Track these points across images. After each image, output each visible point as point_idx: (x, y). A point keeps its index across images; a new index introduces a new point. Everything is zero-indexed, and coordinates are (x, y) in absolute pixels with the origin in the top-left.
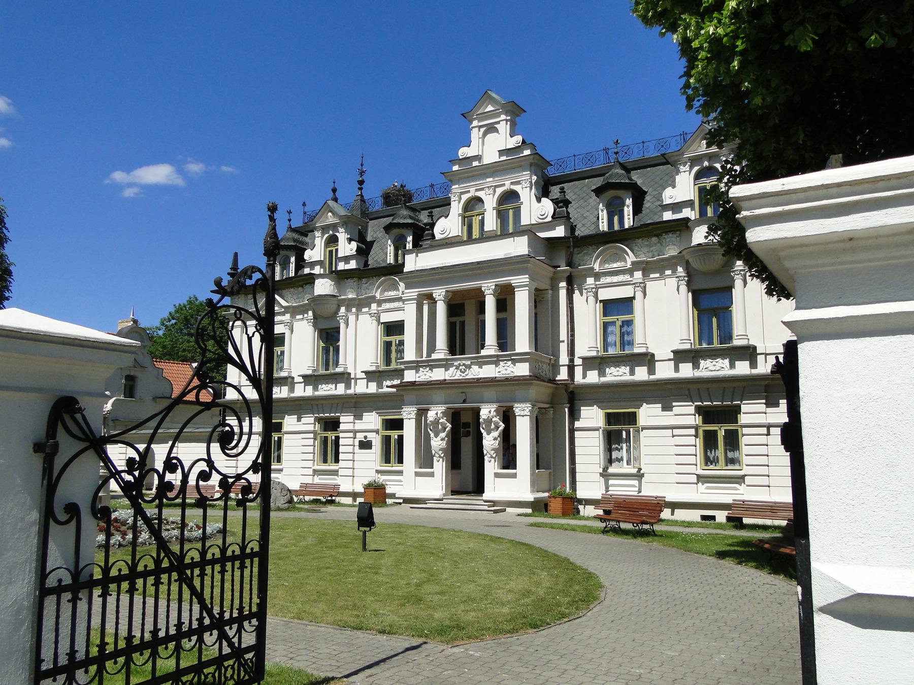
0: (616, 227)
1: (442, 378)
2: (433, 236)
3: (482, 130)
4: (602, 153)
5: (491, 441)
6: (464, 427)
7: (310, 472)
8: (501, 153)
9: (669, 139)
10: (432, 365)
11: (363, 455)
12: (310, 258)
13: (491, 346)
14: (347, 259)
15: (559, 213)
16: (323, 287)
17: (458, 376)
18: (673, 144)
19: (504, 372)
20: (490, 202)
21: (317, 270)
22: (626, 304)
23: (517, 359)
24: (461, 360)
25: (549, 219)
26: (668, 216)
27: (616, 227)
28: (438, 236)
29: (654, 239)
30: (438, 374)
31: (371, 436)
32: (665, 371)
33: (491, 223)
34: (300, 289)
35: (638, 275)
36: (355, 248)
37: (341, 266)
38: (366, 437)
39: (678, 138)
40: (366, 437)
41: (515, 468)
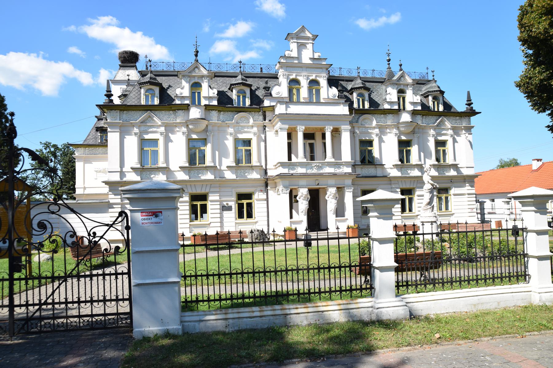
0: (361, 107)
2: (271, 95)
5: (331, 204)
6: (315, 198)
7: (188, 226)
11: (226, 214)
12: (181, 94)
13: (329, 158)
14: (210, 98)
15: (341, 96)
16: (195, 113)
17: (315, 171)
18: (370, 74)
21: (187, 102)
26: (387, 106)
27: (361, 107)
28: (274, 94)
29: (382, 115)
30: (301, 170)
31: (230, 204)
33: (304, 93)
34: (171, 112)
35: (377, 131)
36: (216, 93)
37: (204, 102)
40: (227, 204)
41: (344, 216)
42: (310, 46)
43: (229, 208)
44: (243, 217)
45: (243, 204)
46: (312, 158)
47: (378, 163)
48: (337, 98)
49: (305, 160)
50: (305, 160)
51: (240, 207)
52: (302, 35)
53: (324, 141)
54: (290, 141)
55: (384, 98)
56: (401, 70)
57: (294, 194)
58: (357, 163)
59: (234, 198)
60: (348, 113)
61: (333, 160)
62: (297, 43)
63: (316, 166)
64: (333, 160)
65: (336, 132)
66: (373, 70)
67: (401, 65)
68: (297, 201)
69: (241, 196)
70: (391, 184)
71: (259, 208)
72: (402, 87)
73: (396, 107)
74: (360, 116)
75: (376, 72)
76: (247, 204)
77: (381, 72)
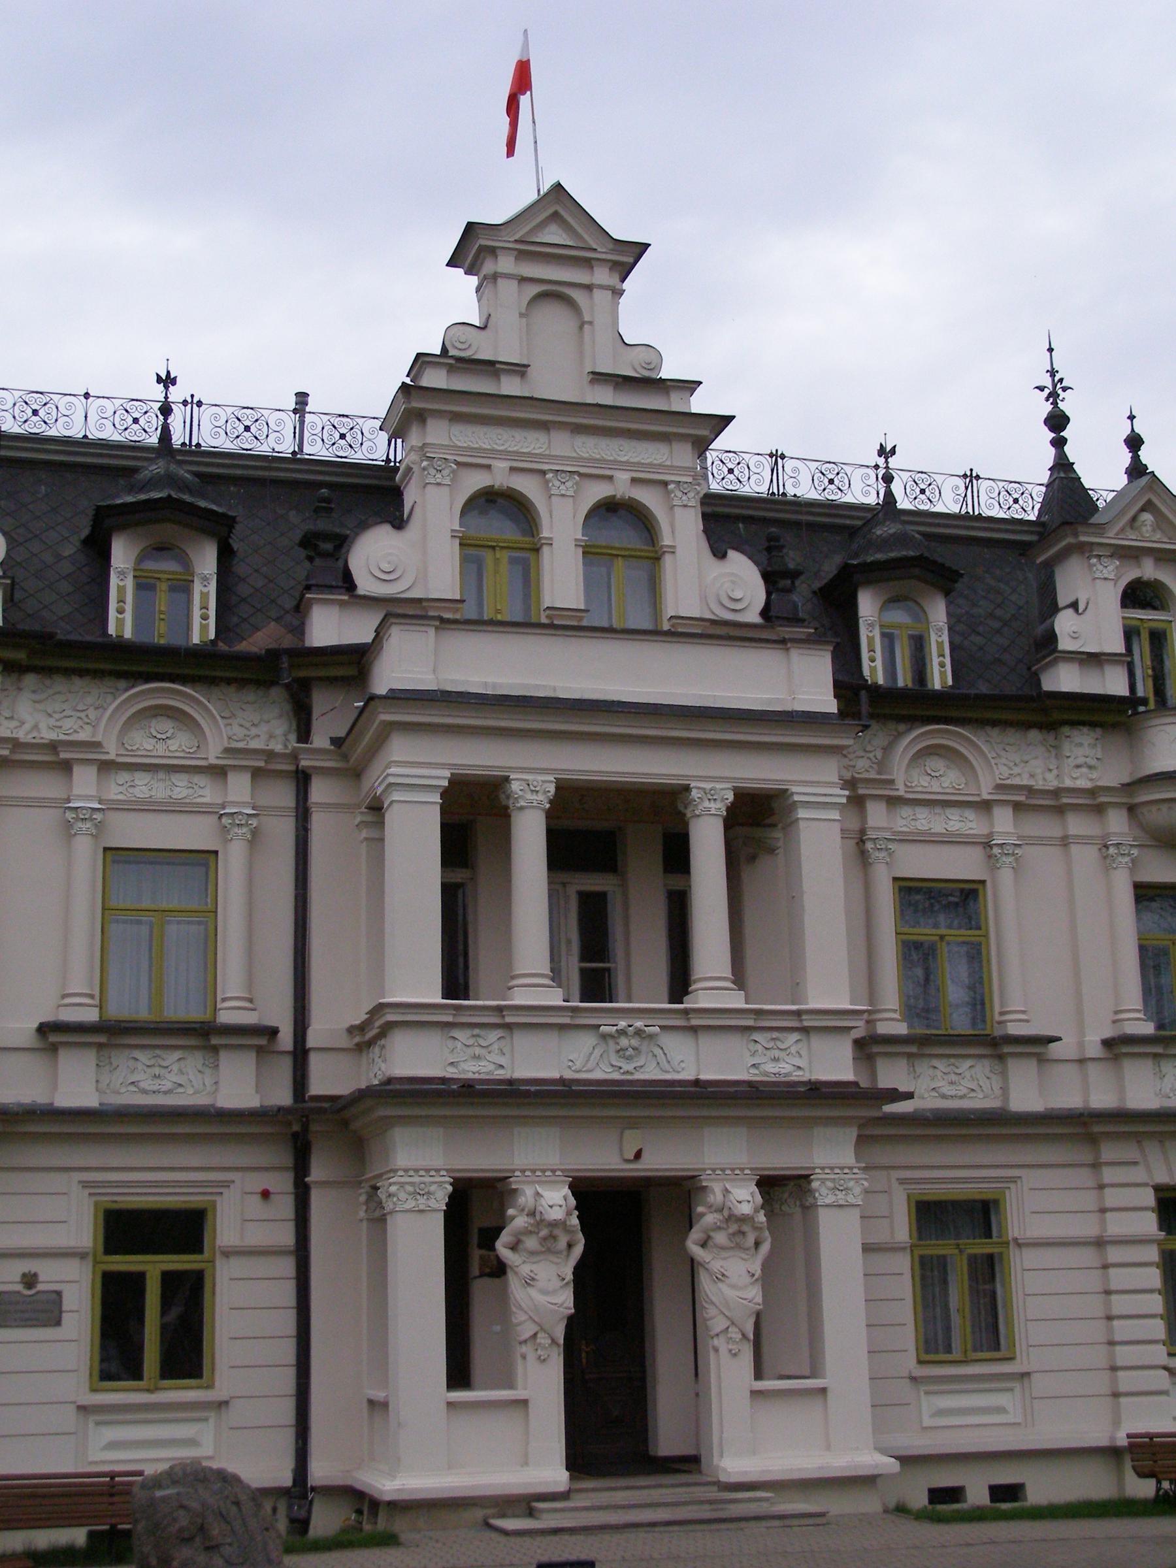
1: (557, 1076)
2: (348, 583)
3: (533, 290)
4: (767, 463)
8: (599, 377)
9: (939, 479)
10: (507, 1022)
18: (948, 495)
19: (771, 1068)
20: (562, 524)
22: (961, 900)
23: (806, 1025)
24: (608, 1017)
25: (753, 616)
28: (365, 585)
29: (1034, 735)
31: (50, 1274)
32: (1066, 1092)
38: (30, 1280)
39: (961, 483)
42: (594, 305)
43: (45, 1311)
44: (137, 1374)
45: (138, 1279)
46: (597, 986)
47: (1014, 1029)
48: (757, 620)
49: (554, 998)
50: (554, 998)
51: (118, 1302)
52: (553, 235)
53: (675, 882)
54: (459, 876)
55: (1040, 629)
56: (1137, 470)
57: (479, 1220)
58: (883, 1029)
59: (82, 1232)
60: (831, 705)
61: (736, 1001)
62: (523, 280)
63: (622, 1032)
64: (736, 1001)
65: (756, 819)
66: (971, 478)
67: (1134, 442)
68: (499, 1270)
69: (125, 1229)
70: (1096, 1166)
71: (244, 1309)
72: (1148, 570)
73: (1115, 684)
74: (900, 735)
75: (984, 485)
76: (169, 1279)
77: (1013, 489)
